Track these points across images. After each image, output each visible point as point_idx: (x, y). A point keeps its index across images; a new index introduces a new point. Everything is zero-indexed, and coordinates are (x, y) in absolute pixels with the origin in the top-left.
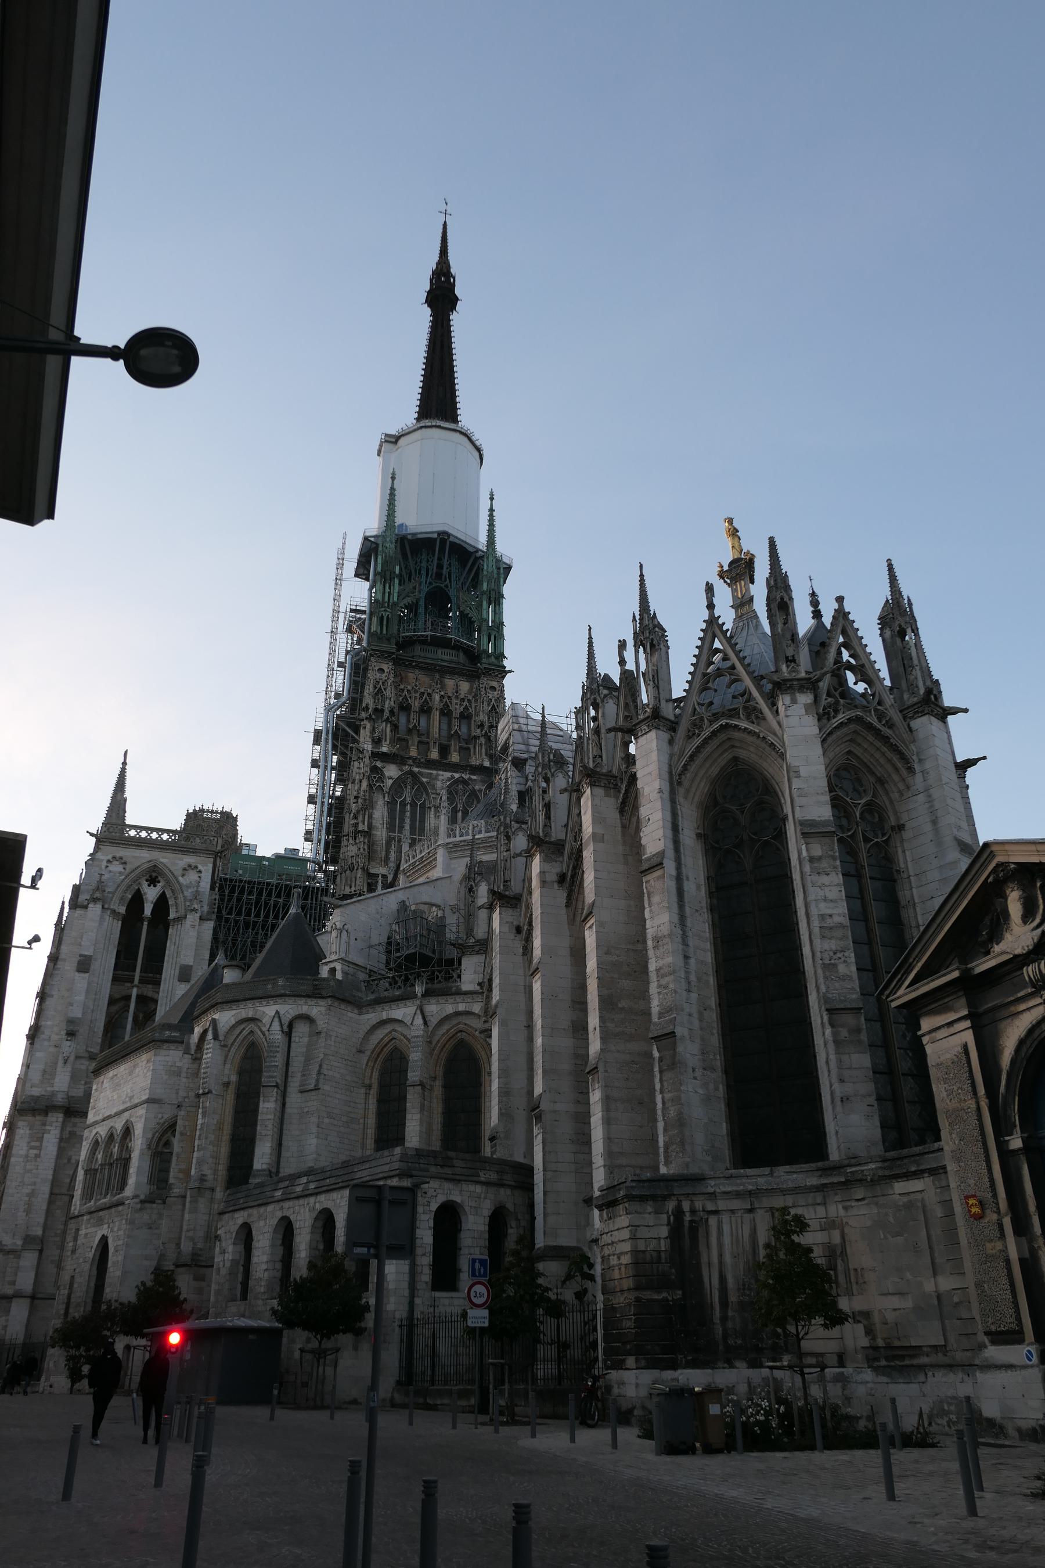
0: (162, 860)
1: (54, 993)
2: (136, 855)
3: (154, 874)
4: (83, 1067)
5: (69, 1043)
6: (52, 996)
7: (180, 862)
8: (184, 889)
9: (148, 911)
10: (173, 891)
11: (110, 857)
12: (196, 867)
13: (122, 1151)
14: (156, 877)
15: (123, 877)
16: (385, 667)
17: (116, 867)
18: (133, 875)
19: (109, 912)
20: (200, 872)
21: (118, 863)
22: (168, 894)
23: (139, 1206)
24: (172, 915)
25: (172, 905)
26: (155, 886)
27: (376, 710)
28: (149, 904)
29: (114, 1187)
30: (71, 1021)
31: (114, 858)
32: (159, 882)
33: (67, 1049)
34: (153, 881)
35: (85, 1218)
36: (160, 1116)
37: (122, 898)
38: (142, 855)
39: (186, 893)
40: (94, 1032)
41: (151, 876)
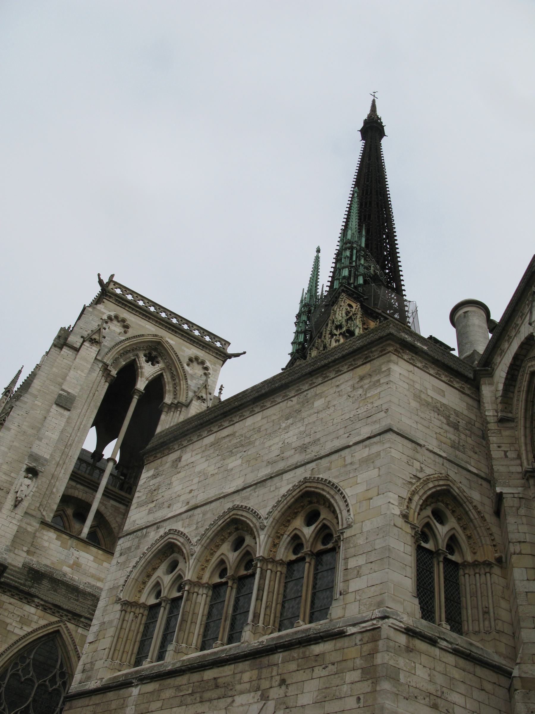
0: (169, 341)
1: (12, 427)
2: (140, 323)
3: (154, 353)
4: (30, 529)
5: (27, 481)
6: (9, 429)
7: (185, 349)
8: (188, 377)
9: (141, 385)
10: (173, 377)
11: (112, 314)
12: (203, 363)
13: (275, 545)
14: (156, 357)
15: (123, 338)
16: (354, 305)
17: (115, 328)
18: (135, 341)
19: (101, 365)
20: (206, 369)
21: (119, 324)
22: (167, 377)
23: (402, 639)
24: (168, 399)
25: (169, 391)
26: (153, 364)
27: (348, 331)
28: (144, 379)
29: (256, 616)
30: (34, 457)
31: (116, 317)
32: (158, 363)
33: (24, 488)
34: (152, 359)
35: (135, 691)
36: (417, 465)
37: (116, 360)
38: (147, 326)
39: (189, 382)
40: (52, 492)
41: (150, 354)
